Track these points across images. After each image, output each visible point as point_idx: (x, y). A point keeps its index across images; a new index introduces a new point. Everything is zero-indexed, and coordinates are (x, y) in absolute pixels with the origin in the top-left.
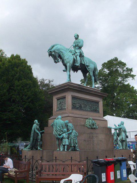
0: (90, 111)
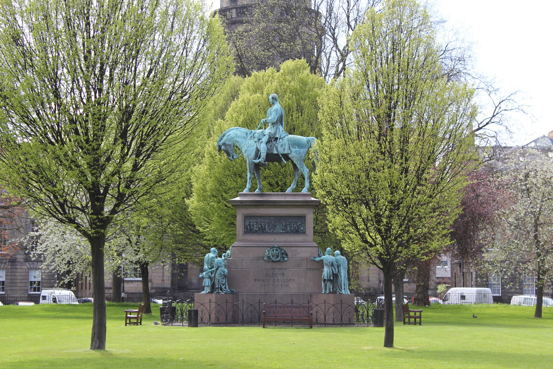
0: (282, 233)
